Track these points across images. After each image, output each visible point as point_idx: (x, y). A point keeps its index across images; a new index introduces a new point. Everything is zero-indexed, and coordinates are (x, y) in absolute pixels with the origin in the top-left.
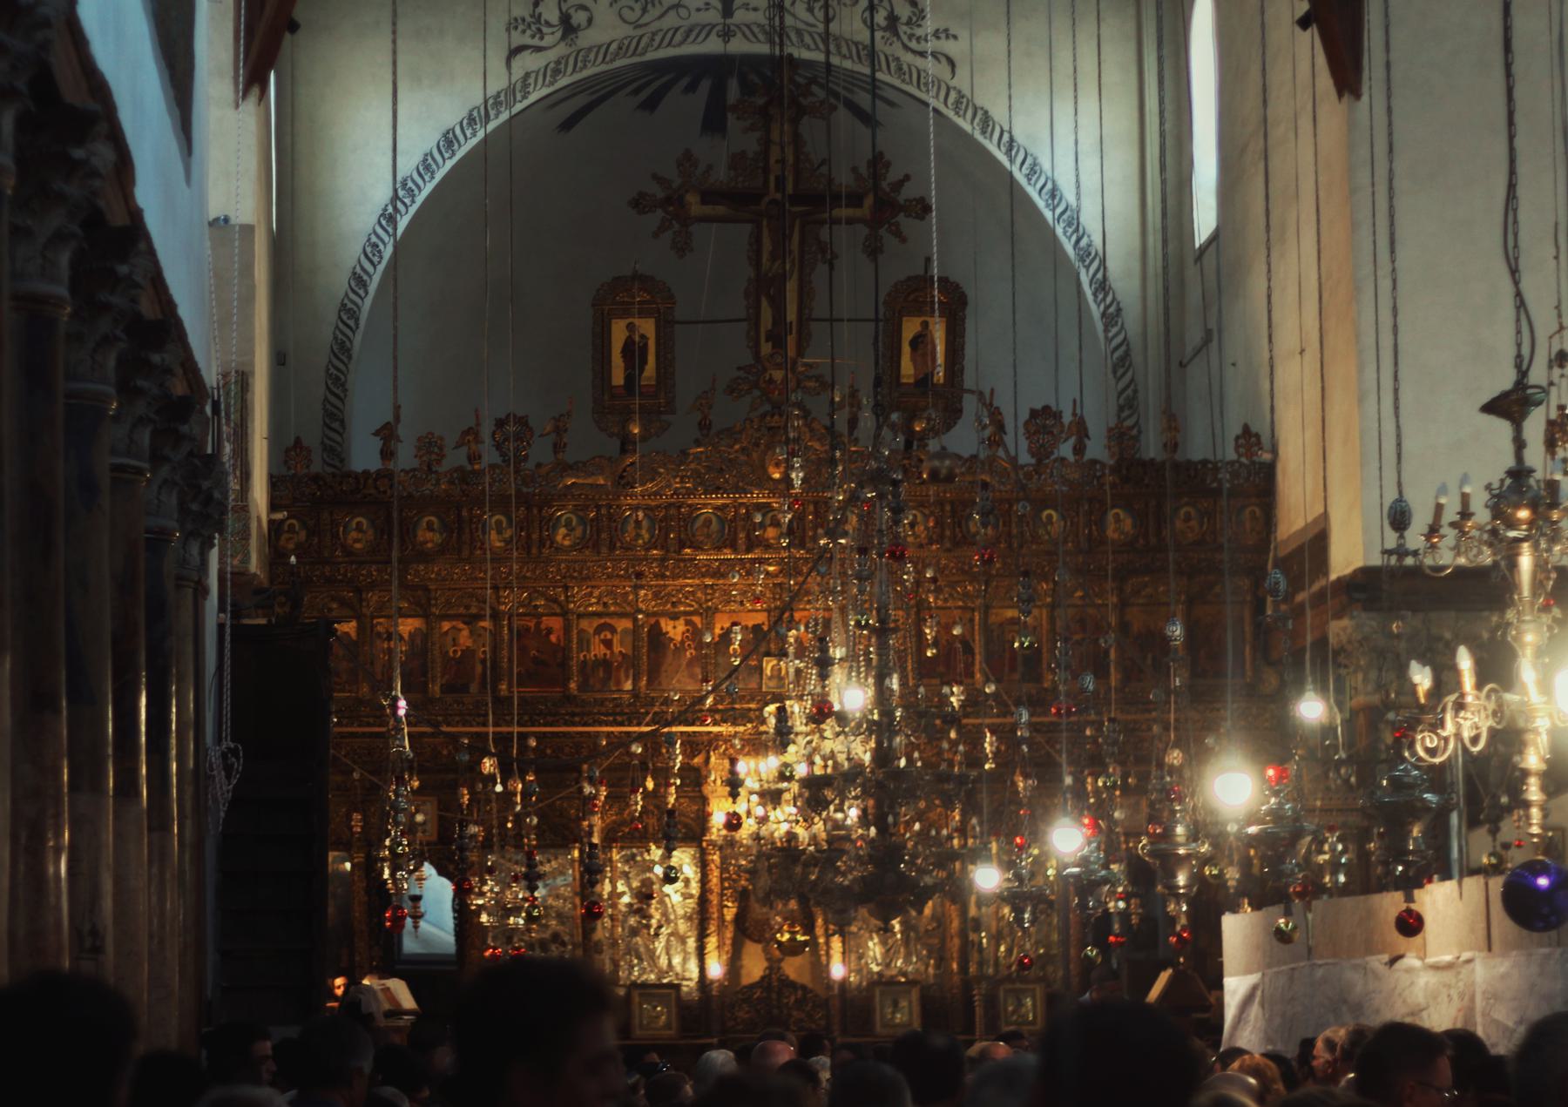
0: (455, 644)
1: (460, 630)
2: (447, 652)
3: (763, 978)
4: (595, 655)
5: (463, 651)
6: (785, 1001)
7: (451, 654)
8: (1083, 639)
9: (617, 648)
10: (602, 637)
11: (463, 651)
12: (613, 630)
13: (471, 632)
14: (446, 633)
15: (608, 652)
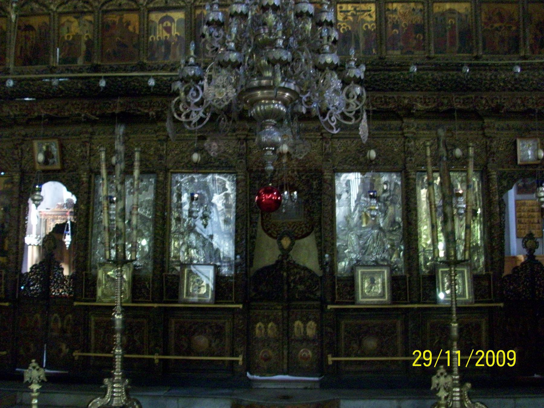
0: (68, 32)
1: (72, 22)
2: (63, 37)
3: (277, 262)
4: (159, 38)
5: (73, 36)
6: (292, 278)
7: (66, 38)
8: (501, 27)
9: (174, 32)
10: (165, 25)
11: (73, 36)
12: (172, 20)
13: (79, 24)
14: (63, 25)
15: (168, 35)
